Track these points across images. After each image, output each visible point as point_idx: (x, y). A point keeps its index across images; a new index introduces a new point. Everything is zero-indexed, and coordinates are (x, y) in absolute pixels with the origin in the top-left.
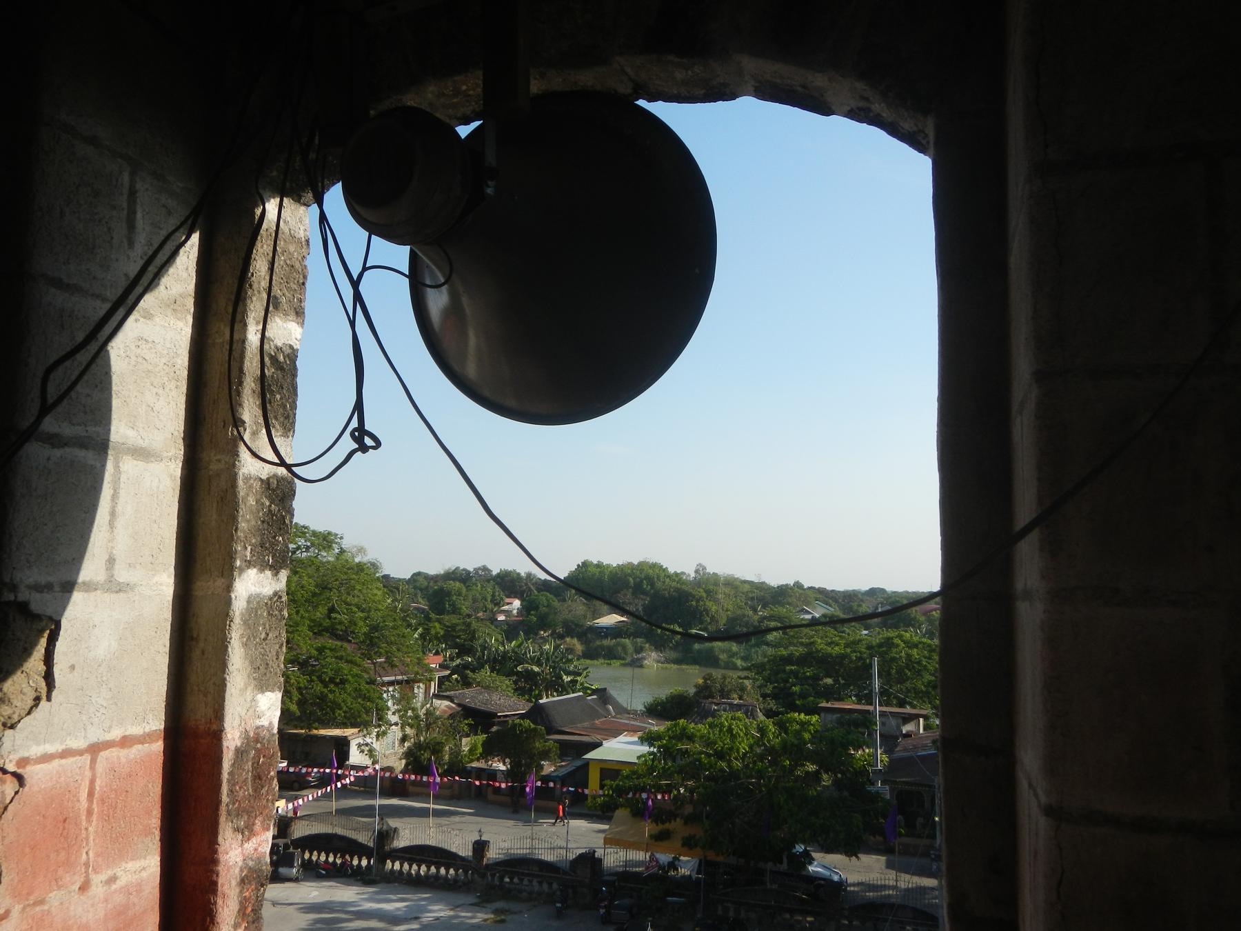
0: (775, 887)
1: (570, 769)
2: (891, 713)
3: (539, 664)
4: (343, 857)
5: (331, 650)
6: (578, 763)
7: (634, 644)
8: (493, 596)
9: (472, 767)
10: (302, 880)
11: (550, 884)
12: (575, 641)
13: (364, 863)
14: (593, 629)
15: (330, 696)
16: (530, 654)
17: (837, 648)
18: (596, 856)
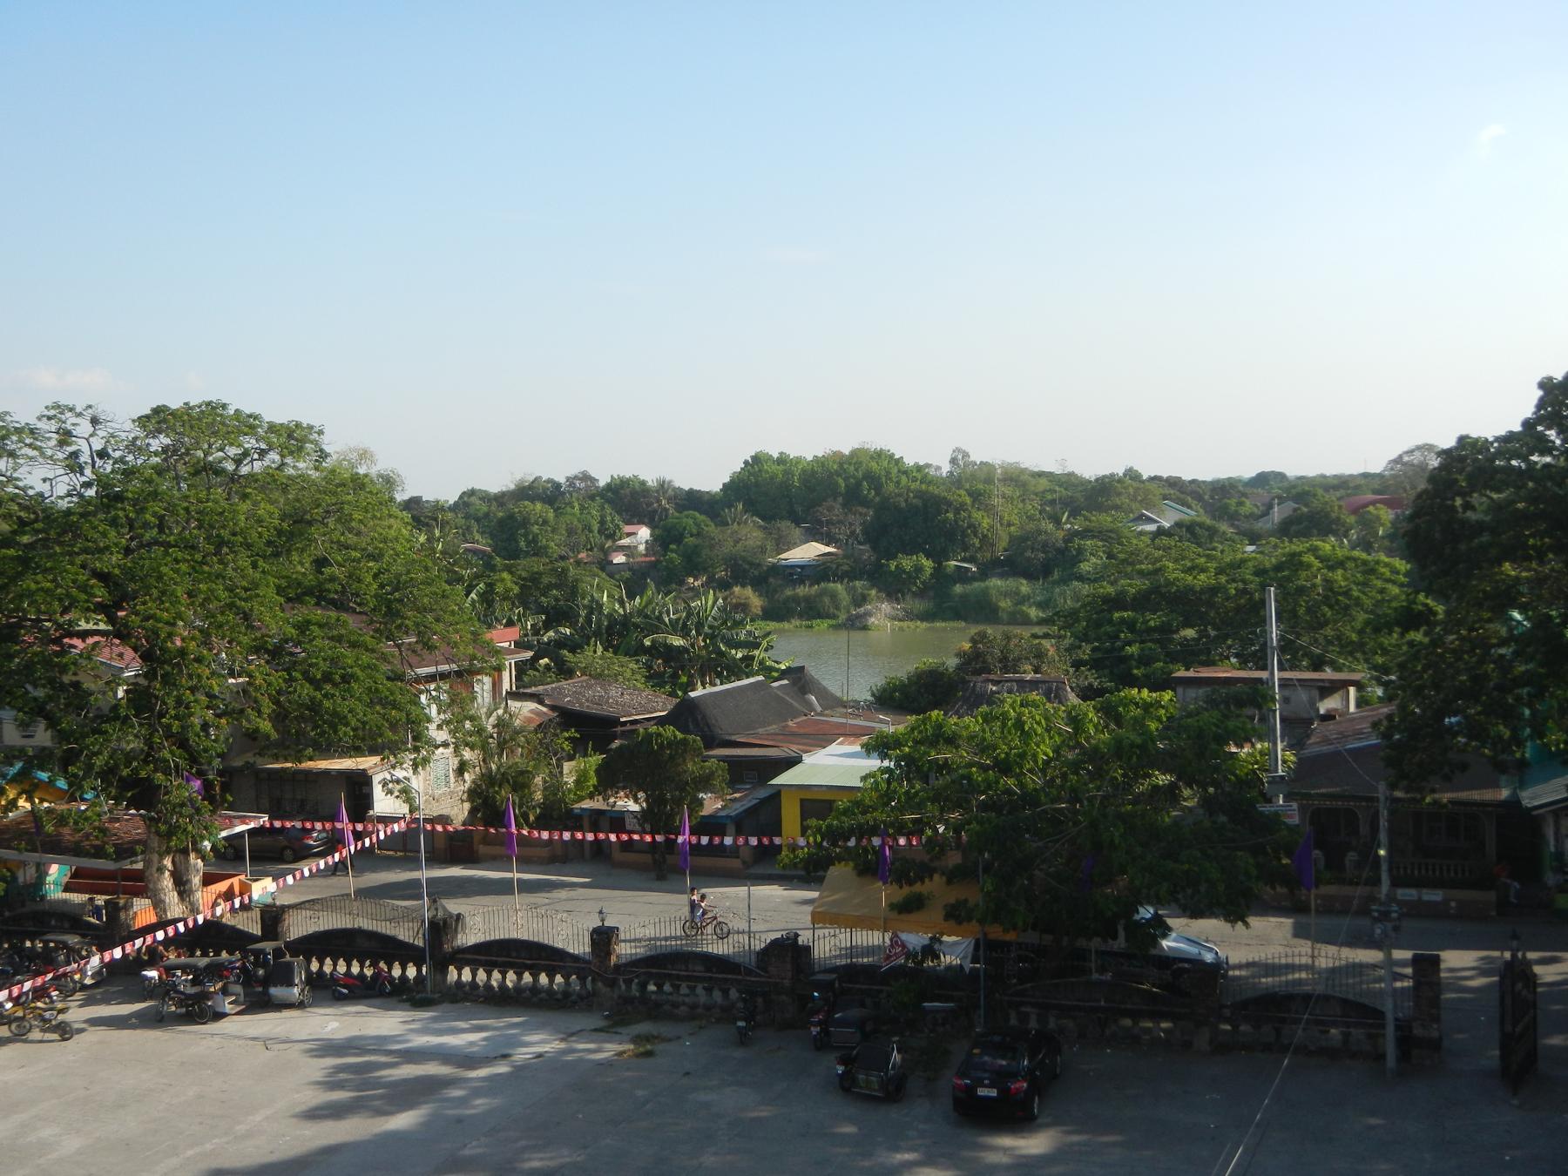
0: (1108, 976)
1: (747, 804)
2: (1299, 680)
3: (685, 633)
4: (374, 965)
5: (320, 626)
6: (762, 793)
8: (602, 522)
9: (582, 809)
10: (310, 1006)
11: (725, 992)
12: (749, 592)
13: (411, 972)
14: (776, 570)
15: (327, 704)
16: (669, 616)
17: (1202, 577)
18: (800, 943)
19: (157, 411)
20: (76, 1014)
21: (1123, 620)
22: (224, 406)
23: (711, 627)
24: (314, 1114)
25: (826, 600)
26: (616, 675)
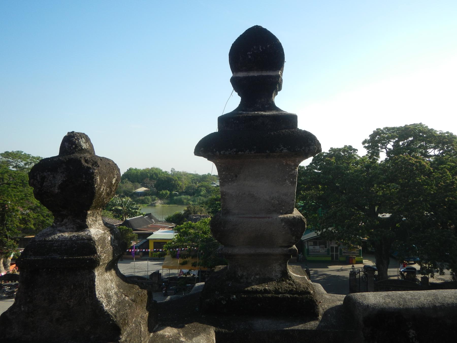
1: (141, 243)
3: (121, 206)
6: (144, 241)
7: (151, 198)
14: (135, 193)
15: (47, 221)
16: (118, 202)
18: (160, 273)
19: (6, 152)
21: (218, 203)
22: (22, 152)
23: (127, 205)
25: (146, 200)
26: (106, 216)
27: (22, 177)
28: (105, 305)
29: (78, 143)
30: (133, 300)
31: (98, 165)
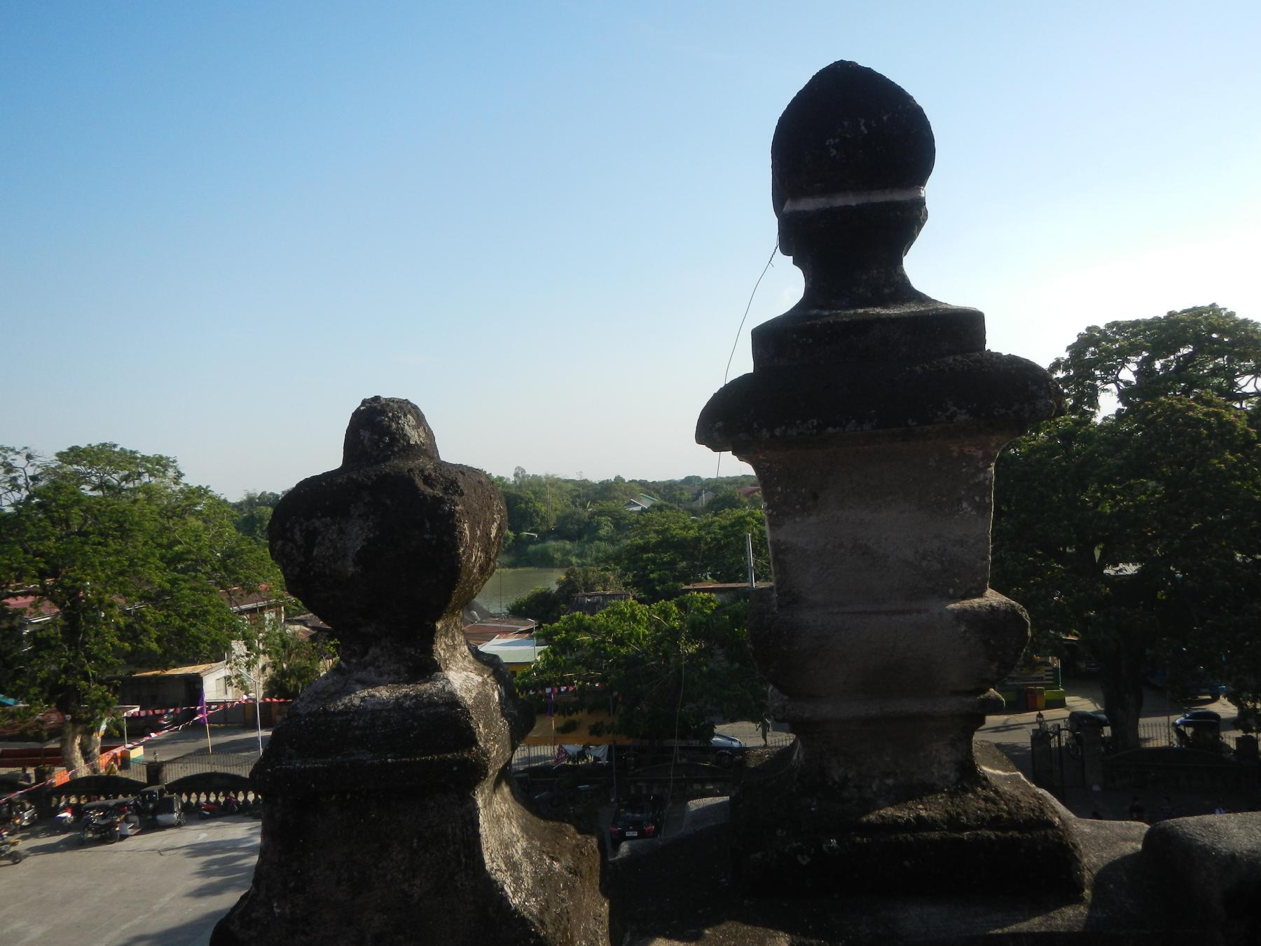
0: (684, 760)
10: (185, 824)
13: (251, 797)
15: (193, 630)
19: (72, 449)
20: (22, 846)
22: (115, 446)
24: (200, 893)
27: (120, 515)
28: (512, 892)
29: (397, 429)
30: (571, 869)
31: (461, 490)
